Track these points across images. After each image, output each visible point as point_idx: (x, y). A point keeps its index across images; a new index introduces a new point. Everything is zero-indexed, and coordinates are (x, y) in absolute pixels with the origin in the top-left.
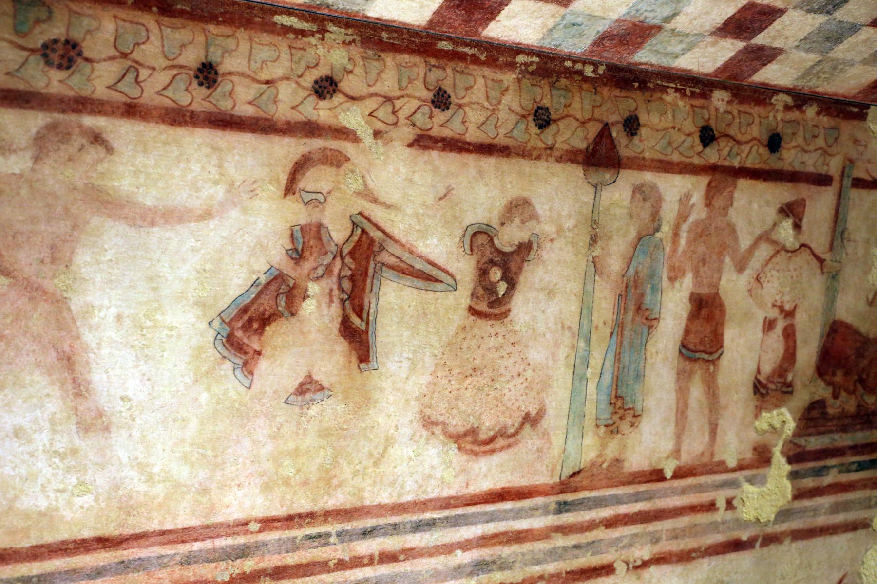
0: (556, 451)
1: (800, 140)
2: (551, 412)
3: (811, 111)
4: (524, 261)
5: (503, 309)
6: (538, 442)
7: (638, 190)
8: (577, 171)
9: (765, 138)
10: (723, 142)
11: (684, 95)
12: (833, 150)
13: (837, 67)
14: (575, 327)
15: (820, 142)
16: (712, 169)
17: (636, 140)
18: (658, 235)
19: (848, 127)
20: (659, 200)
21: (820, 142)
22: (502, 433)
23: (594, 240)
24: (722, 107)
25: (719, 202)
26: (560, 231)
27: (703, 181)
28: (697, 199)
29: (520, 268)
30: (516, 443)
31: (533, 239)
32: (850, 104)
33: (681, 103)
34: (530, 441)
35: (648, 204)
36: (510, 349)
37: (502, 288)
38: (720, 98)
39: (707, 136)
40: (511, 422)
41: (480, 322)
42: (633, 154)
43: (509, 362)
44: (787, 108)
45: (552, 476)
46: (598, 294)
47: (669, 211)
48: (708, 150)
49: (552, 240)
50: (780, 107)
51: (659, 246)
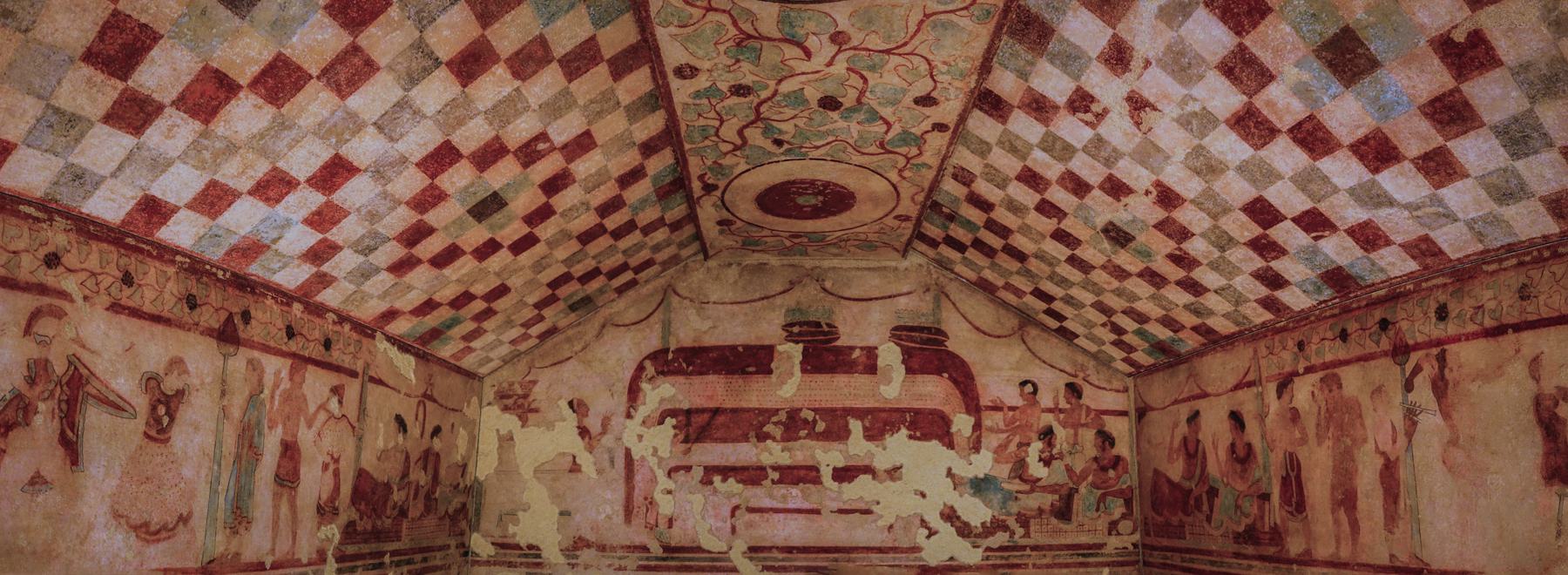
0: (199, 543)
1: (342, 346)
2: (196, 515)
3: (347, 327)
4: (180, 402)
5: (166, 436)
6: (188, 536)
7: (250, 362)
8: (214, 343)
9: (323, 340)
10: (299, 338)
11: (277, 302)
12: (358, 356)
13: (365, 297)
14: (212, 454)
15: (352, 349)
16: (293, 355)
17: (249, 327)
18: (262, 396)
19: (365, 341)
20: (263, 371)
21: (352, 349)
22: (164, 528)
23: (223, 393)
24: (299, 315)
25: (297, 378)
26: (203, 383)
27: (289, 362)
28: (284, 374)
29: (178, 408)
30: (174, 535)
31: (186, 387)
32: (367, 327)
33: (275, 307)
34: (182, 534)
35: (255, 374)
36: (171, 466)
37: (166, 420)
38: (297, 308)
39: (290, 333)
40: (171, 520)
41: (152, 444)
42: (246, 337)
43: (170, 475)
44: (334, 323)
45: (196, 562)
46: (225, 432)
47: (269, 380)
48: (291, 342)
49: (197, 390)
50: (330, 321)
51: (262, 403)
